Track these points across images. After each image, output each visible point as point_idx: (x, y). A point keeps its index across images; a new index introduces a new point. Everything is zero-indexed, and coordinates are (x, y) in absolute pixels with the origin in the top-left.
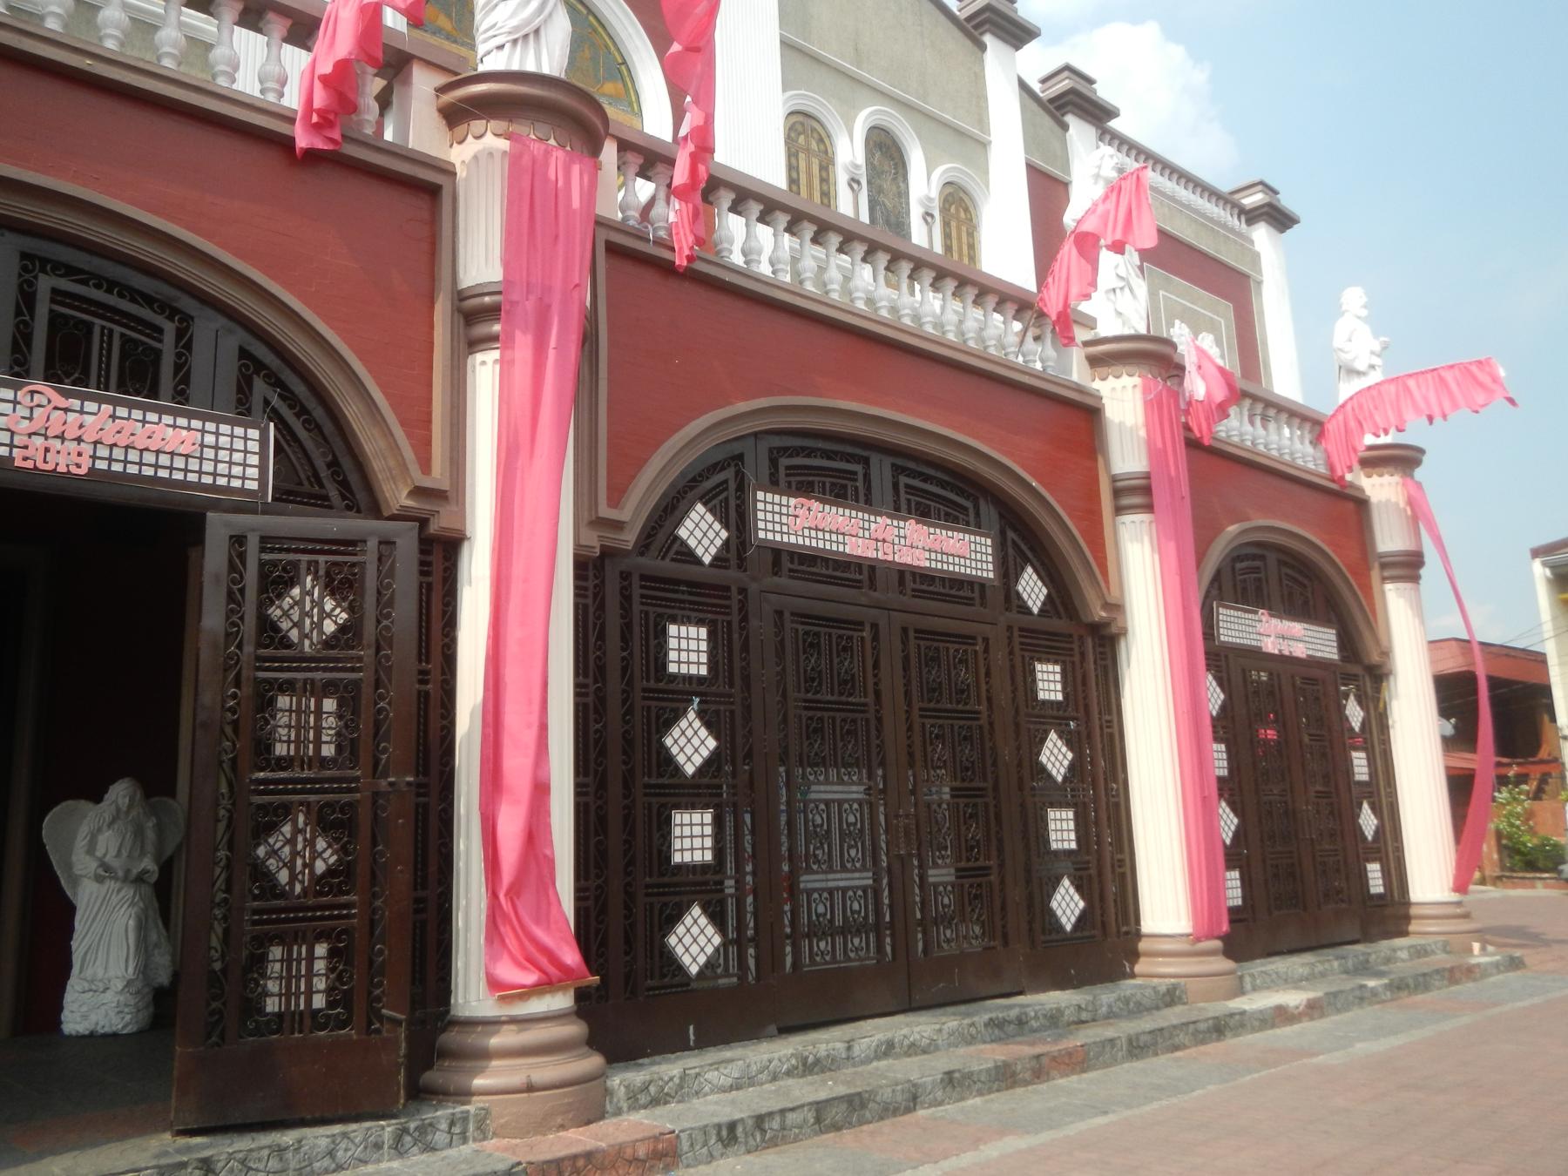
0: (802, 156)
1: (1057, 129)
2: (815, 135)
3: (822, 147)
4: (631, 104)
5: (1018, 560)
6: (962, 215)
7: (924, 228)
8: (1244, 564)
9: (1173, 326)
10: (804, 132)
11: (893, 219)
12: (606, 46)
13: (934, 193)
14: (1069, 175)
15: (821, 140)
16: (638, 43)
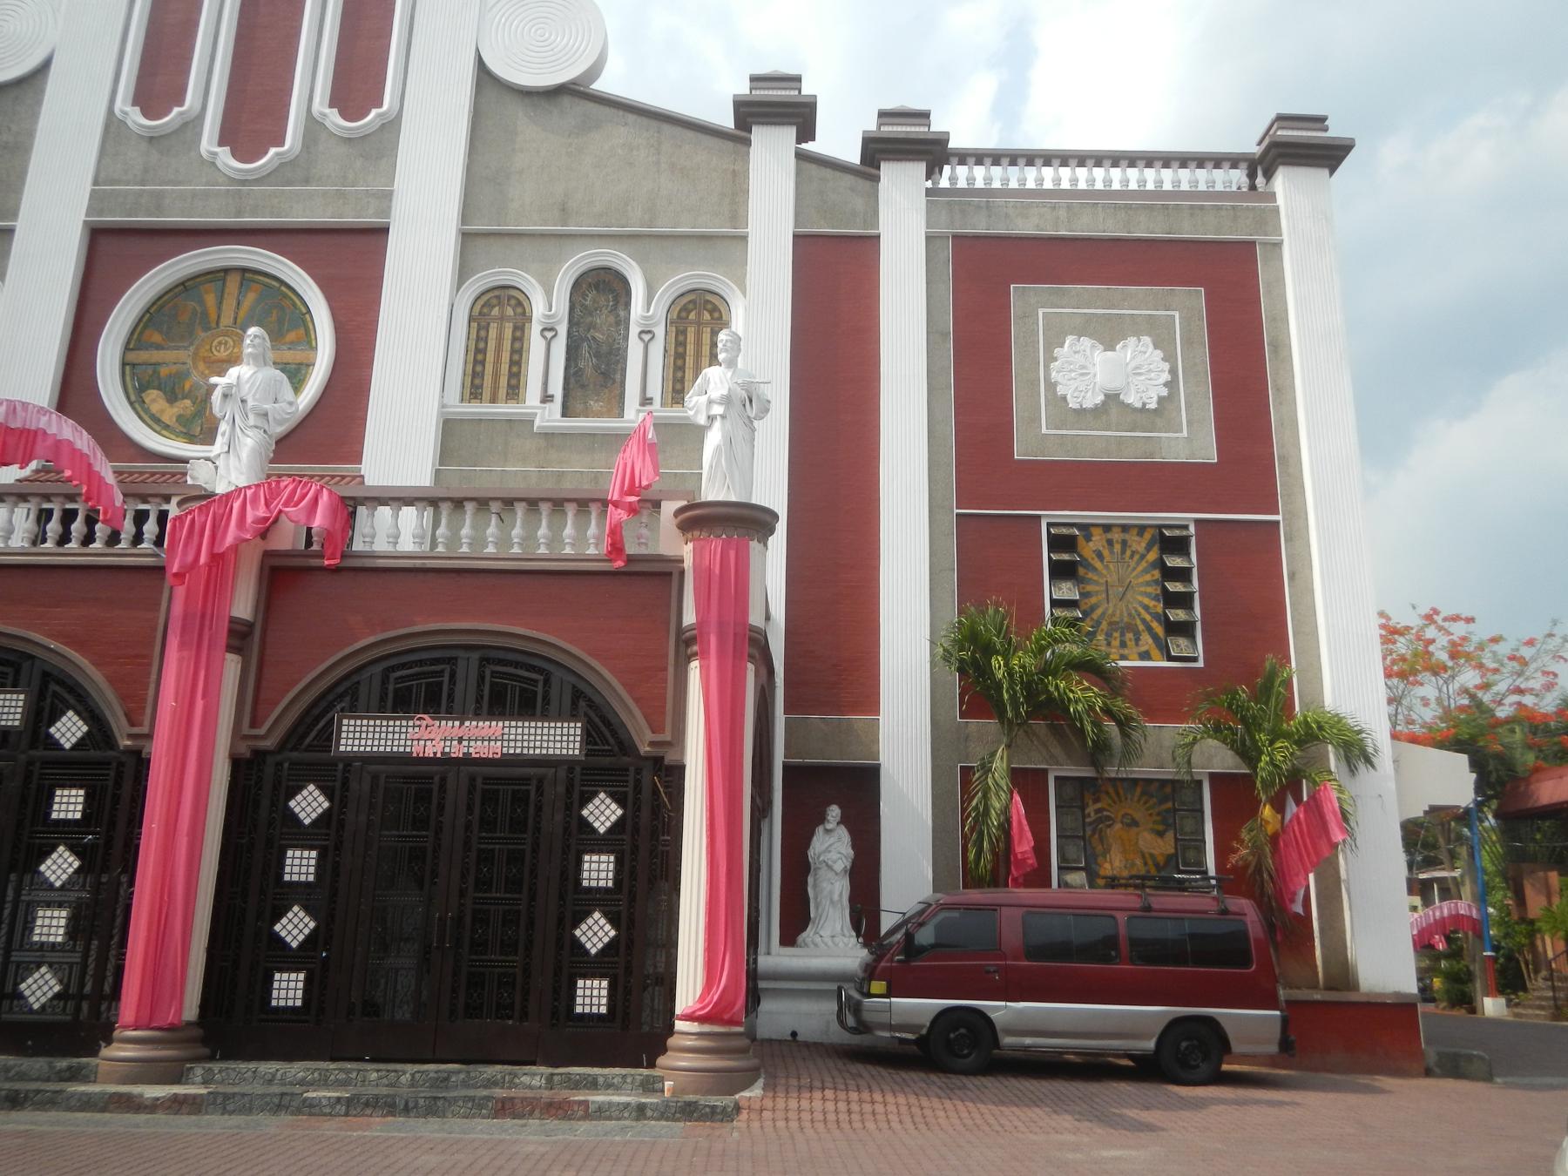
0: (493, 326)
1: (863, 184)
2: (513, 302)
3: (519, 310)
4: (309, 342)
5: (61, 706)
6: (707, 316)
7: (641, 345)
8: (399, 674)
9: (1062, 347)
10: (499, 304)
11: (604, 348)
12: (294, 304)
13: (659, 309)
14: (876, 225)
15: (520, 304)
16: (309, 293)
